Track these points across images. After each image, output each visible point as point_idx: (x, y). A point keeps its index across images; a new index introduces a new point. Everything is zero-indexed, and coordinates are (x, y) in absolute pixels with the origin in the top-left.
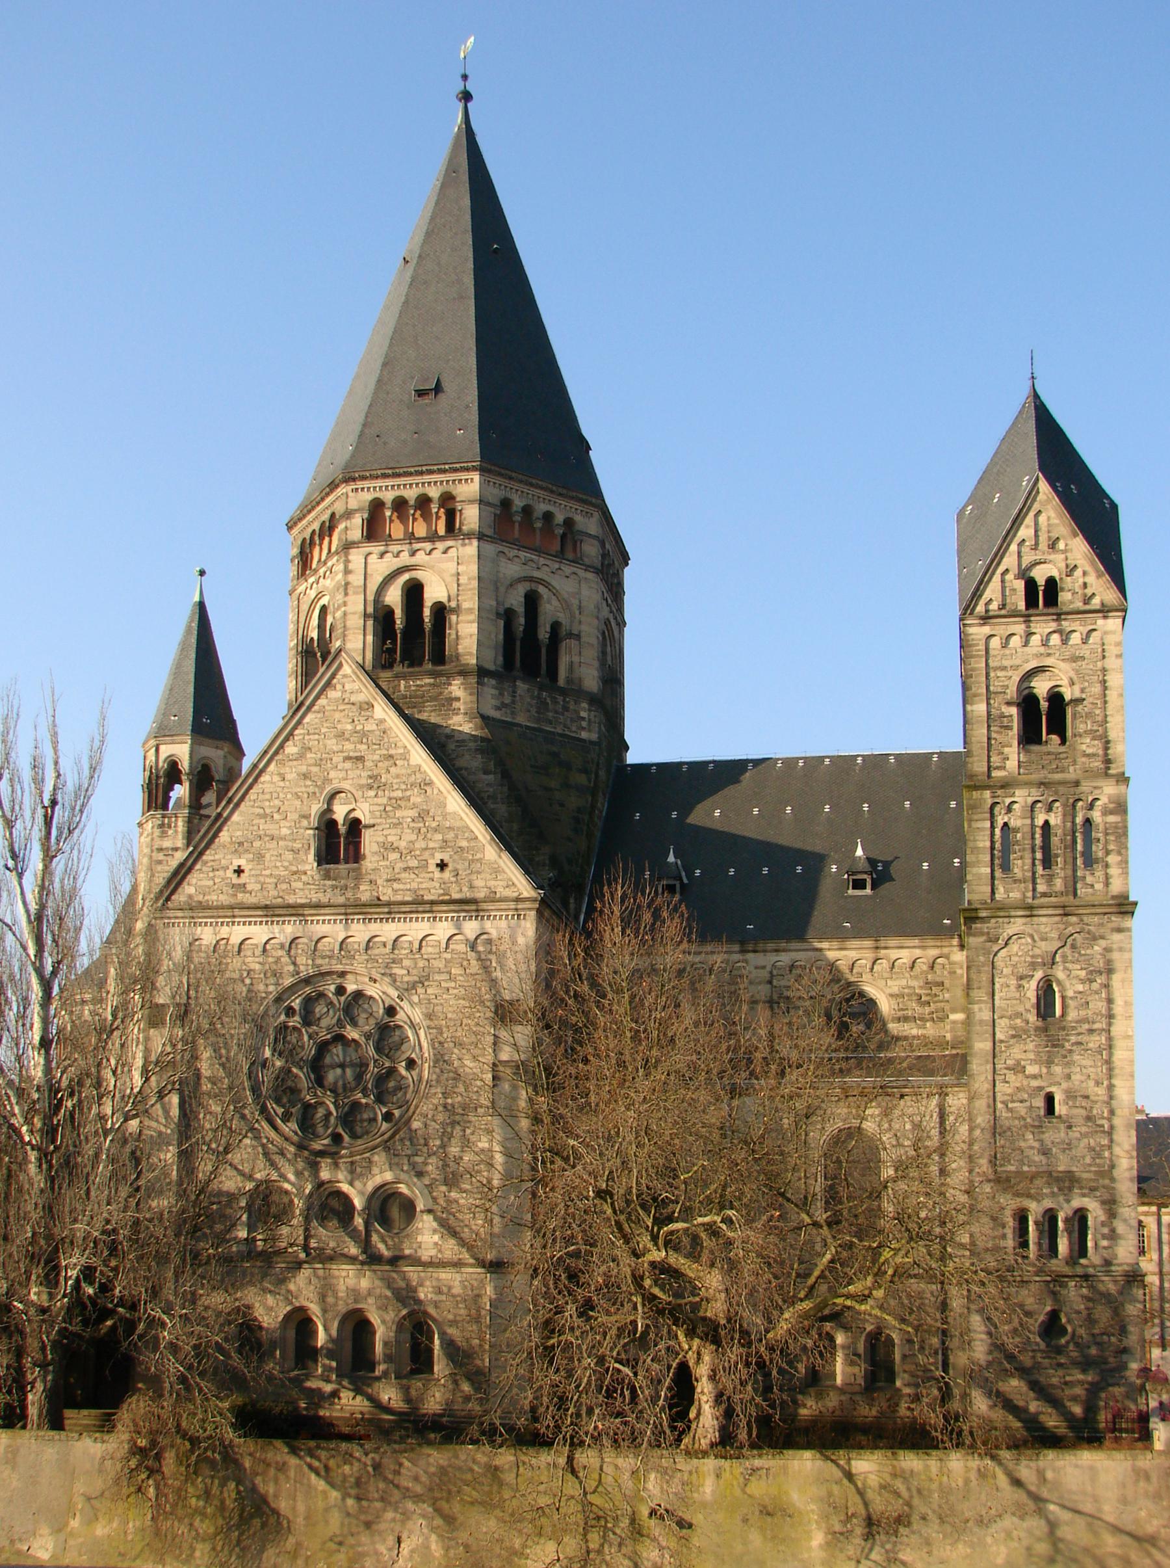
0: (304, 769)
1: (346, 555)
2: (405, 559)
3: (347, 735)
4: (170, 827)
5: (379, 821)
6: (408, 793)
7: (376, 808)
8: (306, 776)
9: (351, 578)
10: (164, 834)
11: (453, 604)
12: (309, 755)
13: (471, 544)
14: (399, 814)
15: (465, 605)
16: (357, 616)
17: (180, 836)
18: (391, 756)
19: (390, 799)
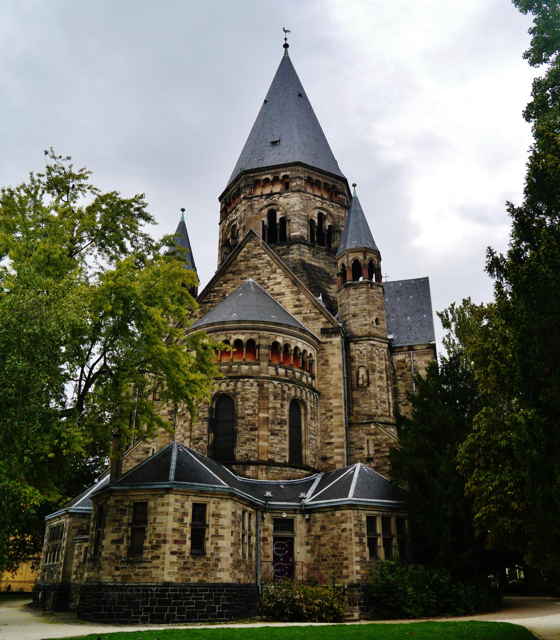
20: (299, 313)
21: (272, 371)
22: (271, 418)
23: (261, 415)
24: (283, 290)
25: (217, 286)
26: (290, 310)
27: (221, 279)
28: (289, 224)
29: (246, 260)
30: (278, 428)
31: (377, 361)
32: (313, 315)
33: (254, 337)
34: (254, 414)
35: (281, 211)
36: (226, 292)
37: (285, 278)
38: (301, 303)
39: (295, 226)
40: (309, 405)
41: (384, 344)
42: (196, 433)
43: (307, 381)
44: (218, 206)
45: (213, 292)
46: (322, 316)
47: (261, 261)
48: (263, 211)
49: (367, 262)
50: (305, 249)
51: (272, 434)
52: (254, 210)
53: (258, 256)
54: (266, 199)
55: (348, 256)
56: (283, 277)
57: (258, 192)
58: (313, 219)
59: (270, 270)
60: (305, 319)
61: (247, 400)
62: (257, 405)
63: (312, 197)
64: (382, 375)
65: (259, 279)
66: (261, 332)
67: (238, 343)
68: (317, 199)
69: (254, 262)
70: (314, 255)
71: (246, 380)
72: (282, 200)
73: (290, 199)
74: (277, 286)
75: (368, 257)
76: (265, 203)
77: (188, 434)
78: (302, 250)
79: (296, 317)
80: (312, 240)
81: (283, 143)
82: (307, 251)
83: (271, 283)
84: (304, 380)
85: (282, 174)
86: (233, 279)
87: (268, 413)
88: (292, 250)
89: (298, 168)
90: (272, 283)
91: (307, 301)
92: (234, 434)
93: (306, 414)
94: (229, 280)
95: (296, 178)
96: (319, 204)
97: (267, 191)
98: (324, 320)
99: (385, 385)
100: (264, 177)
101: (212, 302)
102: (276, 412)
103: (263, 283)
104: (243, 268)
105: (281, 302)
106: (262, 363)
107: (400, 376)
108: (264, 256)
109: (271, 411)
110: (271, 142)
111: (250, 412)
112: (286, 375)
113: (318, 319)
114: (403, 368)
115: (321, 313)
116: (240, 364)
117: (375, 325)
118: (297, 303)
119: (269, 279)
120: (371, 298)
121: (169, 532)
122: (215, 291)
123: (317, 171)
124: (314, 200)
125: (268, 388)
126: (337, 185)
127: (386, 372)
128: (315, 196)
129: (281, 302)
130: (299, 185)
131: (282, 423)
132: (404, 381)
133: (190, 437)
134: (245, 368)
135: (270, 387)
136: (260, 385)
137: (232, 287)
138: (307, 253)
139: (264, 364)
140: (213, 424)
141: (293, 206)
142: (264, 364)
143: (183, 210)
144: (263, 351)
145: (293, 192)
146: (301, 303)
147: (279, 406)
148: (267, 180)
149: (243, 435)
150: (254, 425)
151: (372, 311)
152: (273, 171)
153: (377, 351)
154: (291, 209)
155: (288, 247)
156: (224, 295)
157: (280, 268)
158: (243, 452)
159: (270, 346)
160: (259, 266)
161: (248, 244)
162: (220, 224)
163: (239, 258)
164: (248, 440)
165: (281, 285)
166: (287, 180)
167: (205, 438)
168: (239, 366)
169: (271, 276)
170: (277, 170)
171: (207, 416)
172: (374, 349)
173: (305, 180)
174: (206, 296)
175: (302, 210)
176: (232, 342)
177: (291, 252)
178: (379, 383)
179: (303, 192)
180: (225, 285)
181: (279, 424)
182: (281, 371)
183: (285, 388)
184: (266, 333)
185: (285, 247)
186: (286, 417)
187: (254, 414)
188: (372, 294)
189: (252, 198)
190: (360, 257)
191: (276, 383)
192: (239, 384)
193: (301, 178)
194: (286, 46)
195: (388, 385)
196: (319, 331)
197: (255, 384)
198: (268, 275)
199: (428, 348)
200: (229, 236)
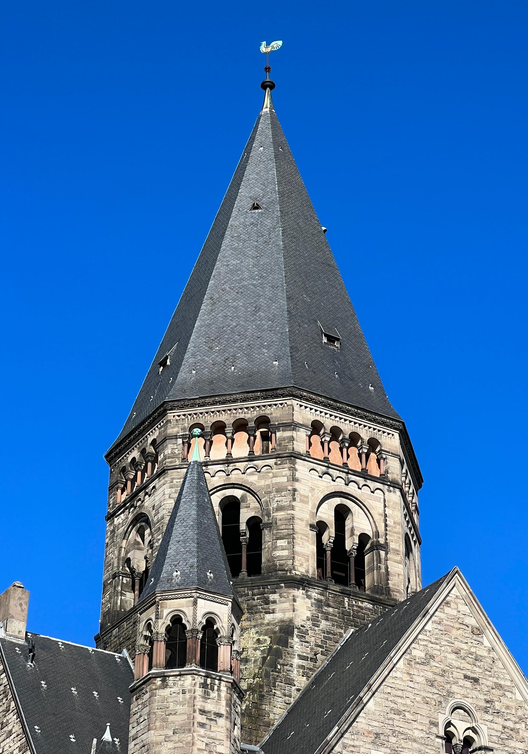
0: (431, 676)
1: (294, 463)
2: (340, 485)
3: (462, 653)
4: (212, 689)
5: (496, 746)
6: (518, 726)
7: (494, 733)
8: (431, 683)
9: (297, 485)
10: (206, 696)
11: (382, 541)
12: (433, 663)
13: (395, 492)
14: (512, 743)
15: (392, 545)
16: (304, 523)
17: (224, 703)
18: (500, 685)
19: (504, 727)
75: (166, 612)
120: (159, 712)
126: (267, 411)
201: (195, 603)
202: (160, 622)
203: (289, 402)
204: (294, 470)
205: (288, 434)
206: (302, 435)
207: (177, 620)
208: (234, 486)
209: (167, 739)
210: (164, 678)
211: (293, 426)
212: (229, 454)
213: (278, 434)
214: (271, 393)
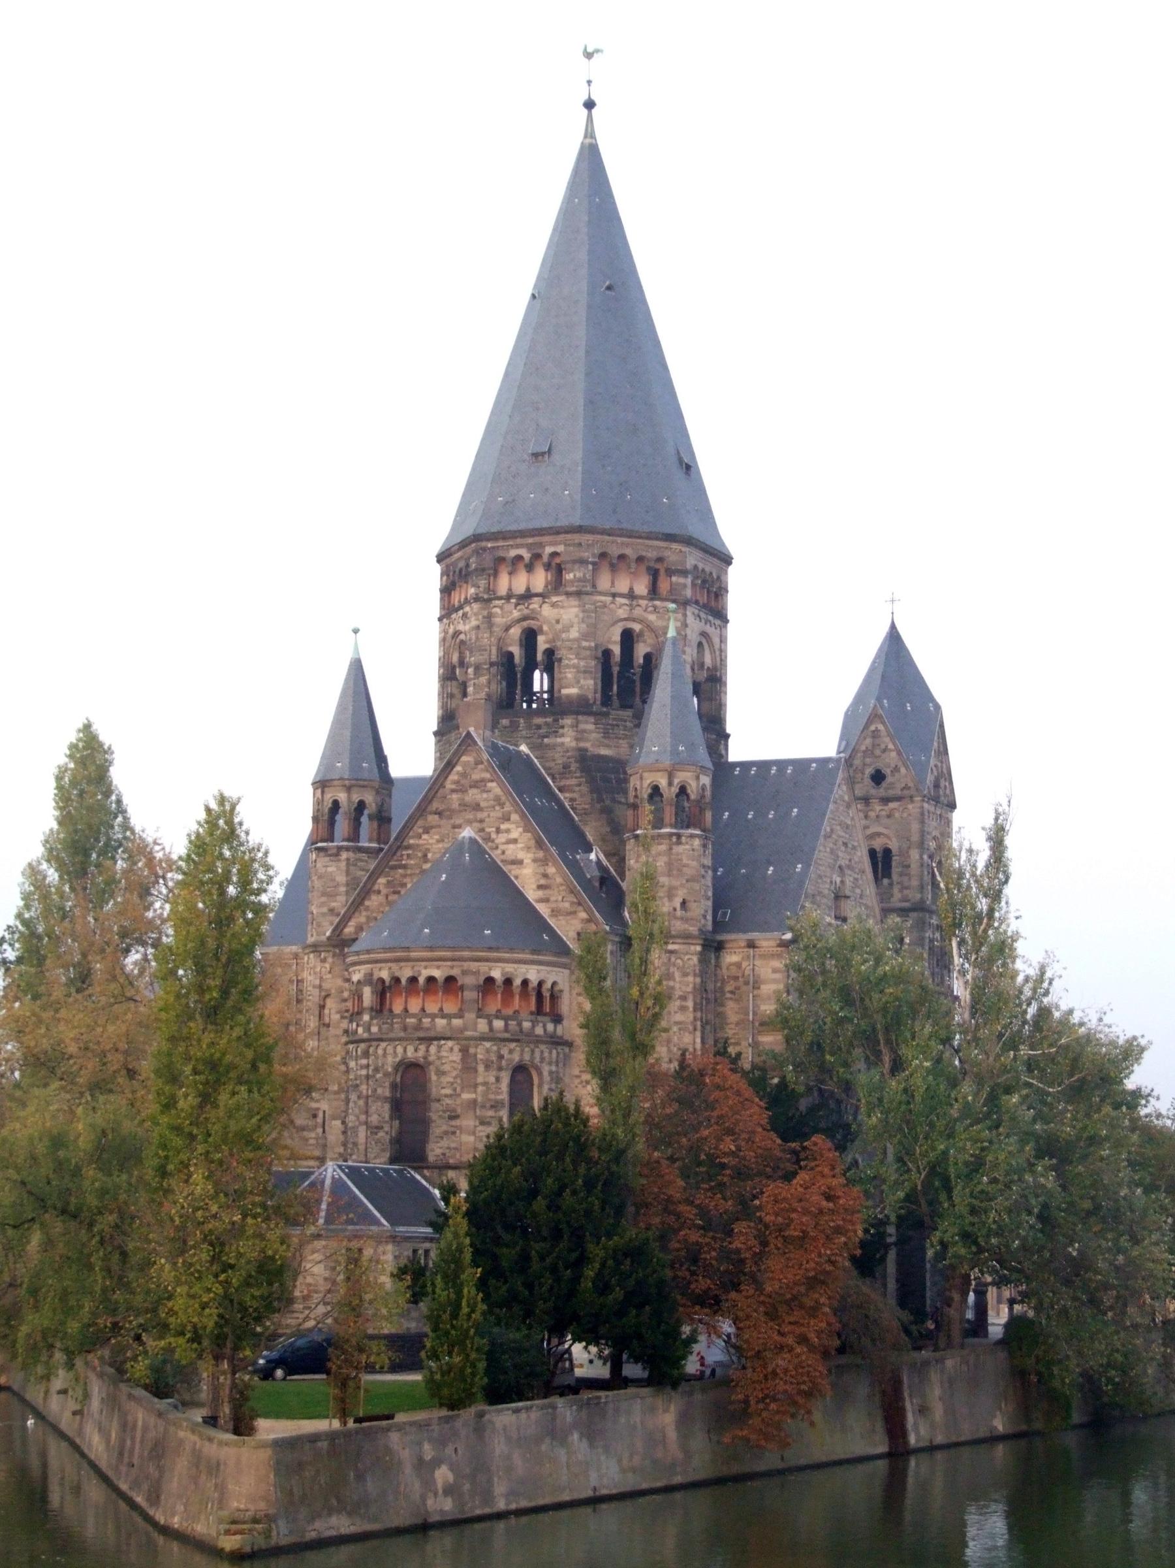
1: (685, 609)
20: (546, 900)
21: (482, 1025)
22: (480, 1099)
23: (466, 1096)
24: (521, 855)
25: (413, 837)
26: (532, 895)
27: (420, 823)
28: (559, 667)
29: (461, 790)
30: (491, 1113)
31: (678, 979)
32: (567, 905)
33: (455, 972)
34: (455, 1095)
35: (546, 634)
36: (428, 850)
37: (524, 831)
38: (549, 881)
39: (570, 675)
40: (546, 1069)
41: (692, 948)
42: (374, 1119)
43: (545, 1030)
44: (433, 576)
45: (408, 847)
46: (581, 908)
47: (485, 795)
48: (512, 631)
49: (675, 790)
50: (588, 724)
51: (482, 1123)
52: (495, 629)
53: (479, 784)
54: (517, 605)
55: (641, 778)
56: (521, 830)
57: (503, 583)
58: (611, 647)
59: (500, 815)
60: (555, 913)
61: (444, 1073)
62: (459, 1081)
63: (609, 599)
64: (684, 1003)
65: (482, 830)
66: (466, 965)
67: (431, 980)
68: (619, 600)
69: (473, 795)
70: (606, 734)
71: (443, 1042)
72: (547, 611)
73: (562, 611)
74: (511, 846)
75: (676, 781)
76: (516, 614)
77: (363, 1117)
78: (582, 726)
79: (543, 909)
80: (606, 700)
81: (556, 457)
82: (591, 727)
83: (501, 838)
84: (539, 1031)
85: (549, 550)
86: (439, 826)
87: (475, 1092)
88: (563, 727)
89: (577, 538)
90: (503, 840)
91: (559, 880)
92: (425, 1123)
93: (540, 1086)
94: (432, 827)
95: (574, 562)
96: (622, 613)
97: (520, 582)
98: (583, 915)
99: (691, 1018)
100: (513, 553)
101: (405, 867)
102: (488, 1089)
103: (488, 839)
104: (455, 806)
105: (516, 877)
106: (467, 1015)
107: (732, 992)
108: (490, 785)
109: (480, 1089)
110: (533, 454)
111: (448, 1091)
112: (506, 1028)
113: (575, 913)
114: (736, 978)
115: (579, 904)
116: (433, 1017)
117: (679, 913)
118: (543, 882)
119: (498, 831)
121: (321, 1282)
122: (408, 847)
123: (620, 536)
124: (612, 606)
125: (475, 1055)
126: (667, 553)
127: (695, 997)
128: (614, 595)
129: (516, 877)
130: (580, 580)
131: (496, 1106)
132: (737, 1001)
133: (366, 1123)
134: (441, 1022)
135: (481, 1051)
136: (464, 1051)
137: (438, 841)
138: (591, 732)
139: (470, 1016)
140: (397, 1106)
141: (566, 629)
142: (470, 1016)
143: (356, 631)
144: (470, 995)
145: (568, 594)
146: (549, 881)
147: (492, 1079)
148: (519, 558)
149: (438, 1126)
150: (454, 1110)
151: (676, 888)
152: (530, 540)
153: (679, 961)
154: (564, 635)
155: (556, 720)
156: (425, 856)
157: (516, 812)
158: (438, 1151)
159: (480, 986)
160: (483, 804)
161: (464, 758)
162: (440, 619)
163: (449, 785)
164: (446, 1133)
165: (520, 845)
166: (558, 560)
167: (387, 1128)
168: (433, 1020)
169: (503, 827)
170: (537, 539)
171: (388, 1094)
172: (673, 959)
173: (594, 564)
174: (395, 853)
175: (585, 636)
176: (421, 980)
177: (561, 731)
178: (679, 1017)
179: (587, 594)
180: (425, 836)
181: (492, 1107)
182: (499, 1024)
183: (505, 1052)
184: (474, 966)
185: (549, 720)
186: (504, 1096)
187: (455, 1095)
188: (678, 854)
189: (489, 600)
190: (663, 782)
191: (488, 1045)
192: (433, 1049)
193: (582, 562)
194: (590, 105)
195: (695, 1019)
196: (573, 934)
197: (456, 1048)
198: (496, 824)
199: (779, 946)
200: (455, 658)
201: (698, 778)
202: (673, 789)
203: (683, 549)
204: (685, 615)
205: (681, 580)
206: (689, 581)
207: (683, 790)
208: (634, 620)
209: (682, 885)
210: (679, 836)
211: (684, 573)
212: (631, 589)
213: (674, 579)
214: (670, 538)
